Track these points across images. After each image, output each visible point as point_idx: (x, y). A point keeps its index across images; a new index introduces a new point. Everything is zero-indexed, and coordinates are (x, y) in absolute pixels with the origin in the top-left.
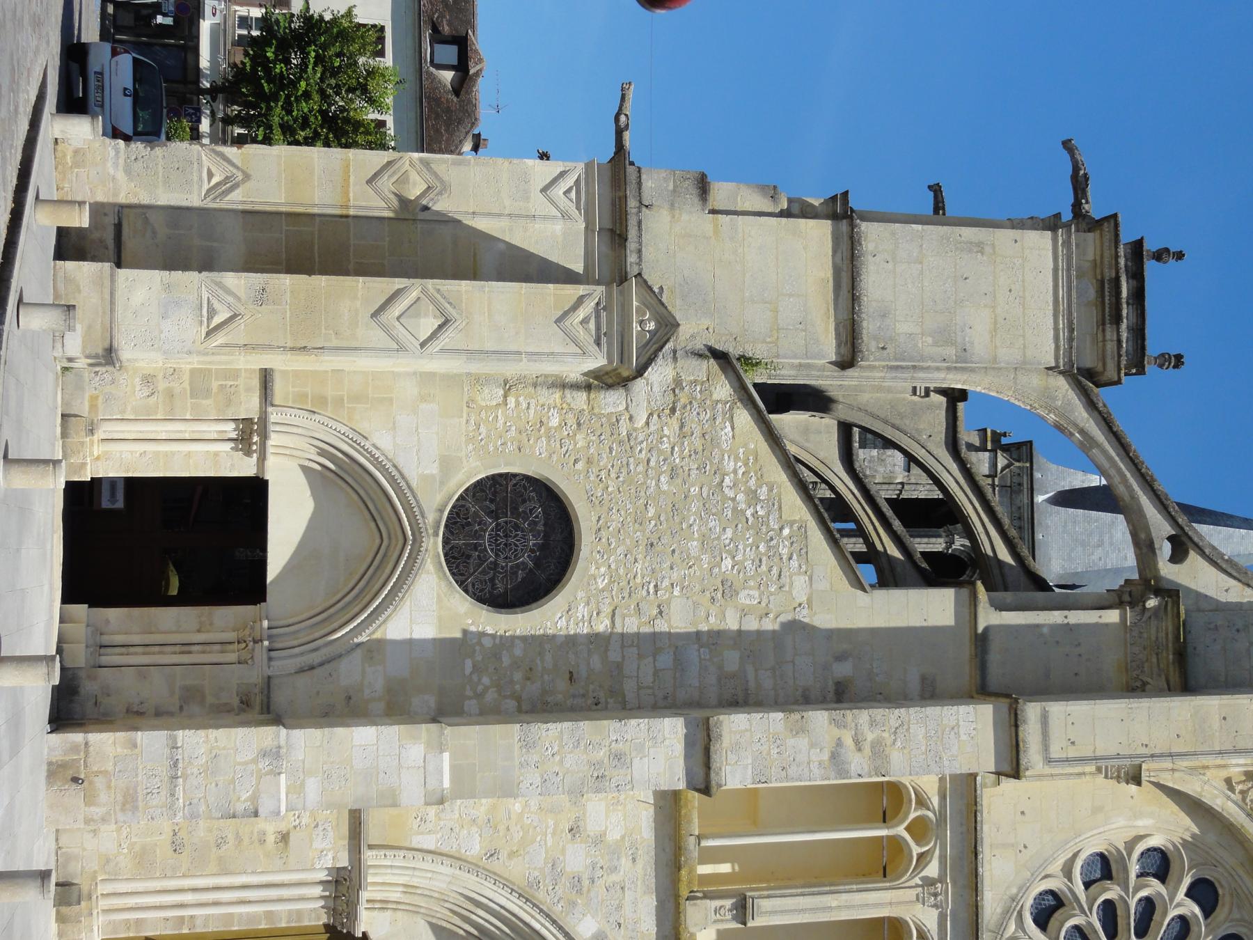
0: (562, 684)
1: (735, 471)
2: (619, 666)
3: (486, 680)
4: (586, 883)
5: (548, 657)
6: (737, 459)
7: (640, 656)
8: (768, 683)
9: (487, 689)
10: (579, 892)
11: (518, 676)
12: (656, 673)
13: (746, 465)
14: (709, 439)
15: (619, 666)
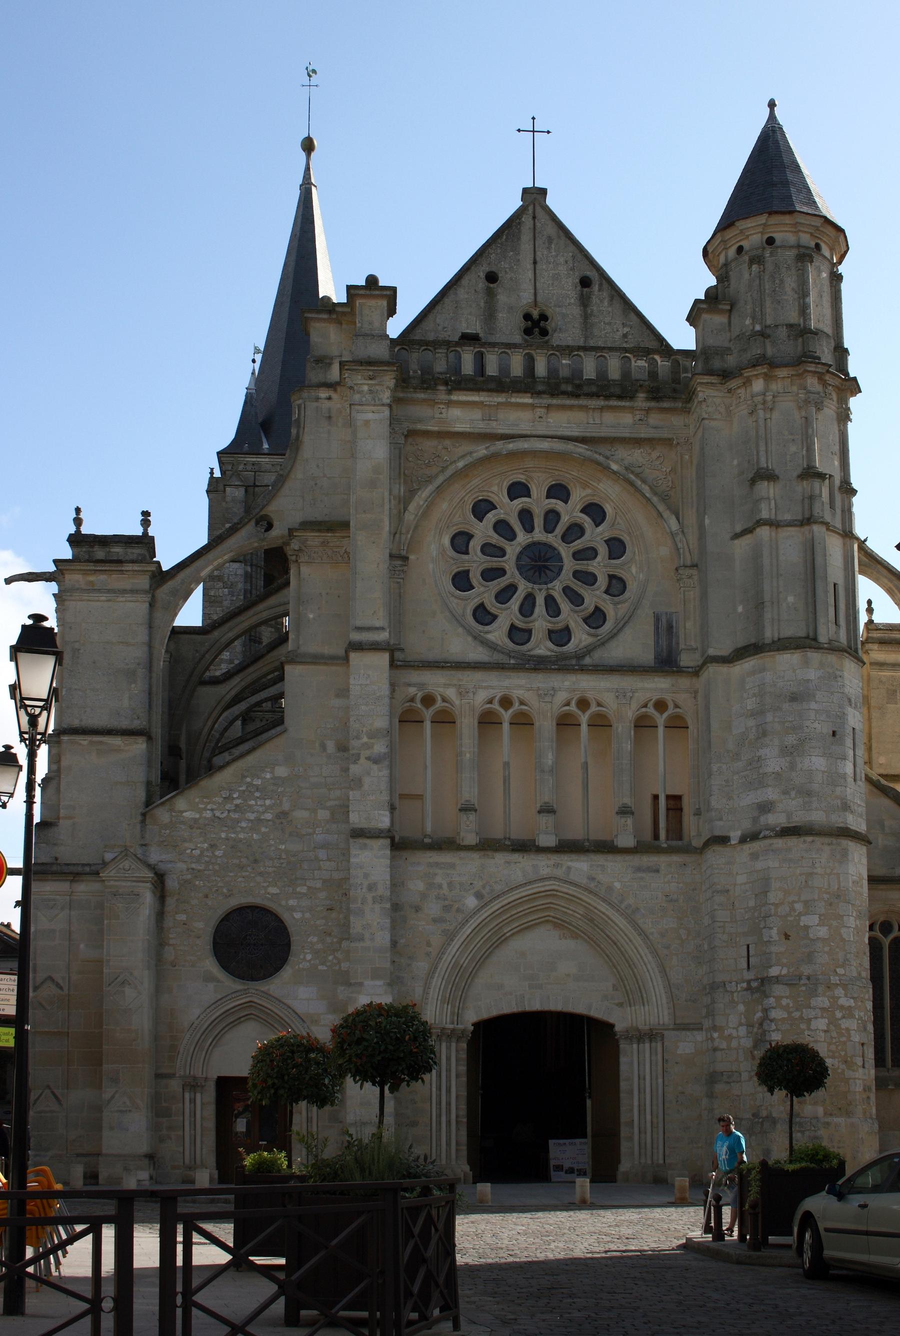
0: (334, 915)
1: (212, 810)
2: (325, 881)
3: (330, 958)
4: (447, 903)
5: (318, 922)
6: (205, 809)
7: (320, 869)
8: (338, 793)
9: (335, 957)
10: (451, 906)
11: (329, 940)
12: (329, 860)
13: (209, 803)
14: (193, 824)
15: (325, 881)
